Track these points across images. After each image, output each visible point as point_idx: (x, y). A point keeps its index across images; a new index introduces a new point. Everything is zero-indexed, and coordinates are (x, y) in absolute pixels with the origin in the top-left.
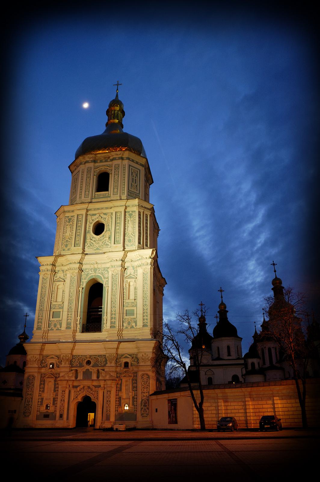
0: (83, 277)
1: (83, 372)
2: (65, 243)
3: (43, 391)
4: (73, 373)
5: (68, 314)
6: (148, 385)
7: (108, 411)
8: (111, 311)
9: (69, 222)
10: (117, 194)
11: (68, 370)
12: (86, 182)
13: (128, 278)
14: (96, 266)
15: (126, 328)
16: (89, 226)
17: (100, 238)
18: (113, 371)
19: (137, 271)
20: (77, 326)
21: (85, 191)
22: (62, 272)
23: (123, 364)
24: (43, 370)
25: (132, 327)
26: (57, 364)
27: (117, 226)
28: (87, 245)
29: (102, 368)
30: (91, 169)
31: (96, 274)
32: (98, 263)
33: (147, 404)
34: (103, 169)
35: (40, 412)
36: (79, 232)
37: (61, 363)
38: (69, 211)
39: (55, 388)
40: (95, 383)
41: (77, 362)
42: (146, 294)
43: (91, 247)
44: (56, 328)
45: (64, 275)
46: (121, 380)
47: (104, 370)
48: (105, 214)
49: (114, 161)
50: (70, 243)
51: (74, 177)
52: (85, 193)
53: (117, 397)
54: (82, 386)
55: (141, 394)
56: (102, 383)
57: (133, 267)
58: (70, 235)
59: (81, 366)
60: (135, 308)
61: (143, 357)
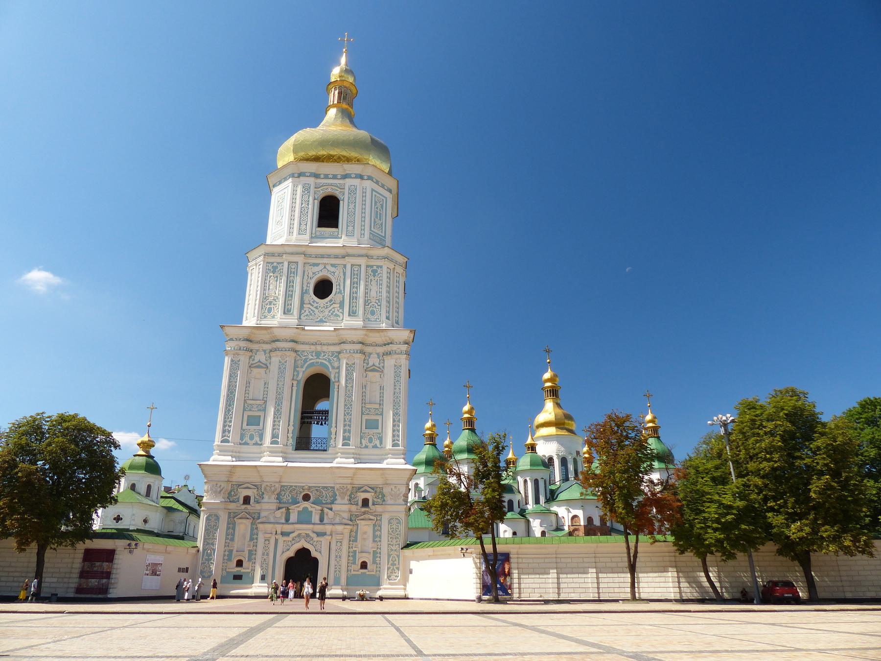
2: (268, 306)
3: (232, 540)
4: (282, 513)
6: (397, 534)
7: (338, 572)
8: (345, 421)
11: (274, 507)
12: (301, 209)
14: (319, 348)
17: (327, 303)
18: (344, 511)
19: (384, 360)
20: (287, 440)
21: (300, 223)
22: (263, 352)
23: (361, 501)
24: (232, 506)
27: (354, 287)
28: (303, 313)
29: (329, 506)
31: (320, 361)
32: (322, 344)
33: (397, 562)
34: (330, 190)
35: (228, 570)
36: (292, 291)
37: (262, 496)
38: (273, 254)
39: (252, 534)
40: (319, 528)
41: (289, 496)
42: (397, 397)
43: (311, 317)
44: (254, 442)
45: (266, 357)
46: (357, 525)
48: (333, 265)
49: (347, 180)
50: (276, 307)
52: (300, 227)
53: (351, 550)
55: (388, 547)
56: (328, 528)
57: (378, 354)
58: (275, 294)
59: (295, 502)
61: (393, 492)
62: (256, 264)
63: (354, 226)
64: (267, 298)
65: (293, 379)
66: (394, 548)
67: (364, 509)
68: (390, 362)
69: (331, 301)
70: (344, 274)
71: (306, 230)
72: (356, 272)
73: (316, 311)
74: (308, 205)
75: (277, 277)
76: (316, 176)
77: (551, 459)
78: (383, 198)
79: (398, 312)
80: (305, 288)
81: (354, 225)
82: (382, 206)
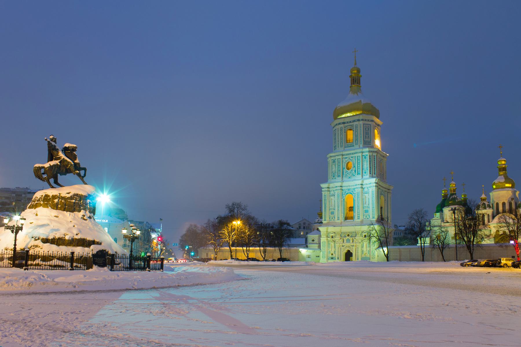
0: (344, 193)
1: (346, 240)
5: (338, 213)
8: (358, 211)
13: (365, 193)
14: (349, 188)
15: (365, 219)
16: (344, 165)
30: (342, 129)
31: (350, 192)
37: (336, 235)
40: (352, 244)
43: (346, 177)
47: (355, 238)
48: (352, 157)
54: (346, 246)
56: (355, 244)
57: (367, 187)
59: (345, 237)
60: (368, 209)
66: (373, 249)
67: (364, 238)
69: (352, 170)
74: (342, 135)
80: (344, 167)
82: (369, 129)
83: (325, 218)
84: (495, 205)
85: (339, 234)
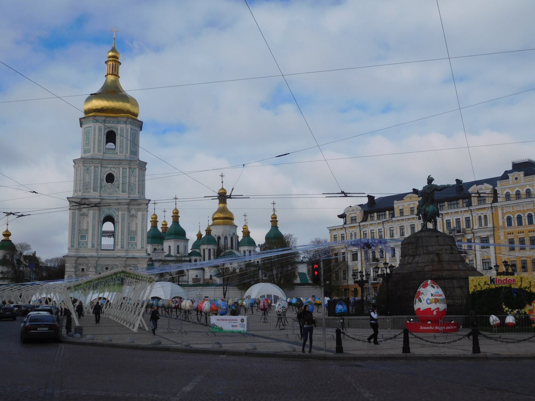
0: (101, 213)
2: (86, 187)
5: (92, 238)
9: (88, 170)
10: (123, 153)
15: (130, 248)
19: (137, 212)
24: (78, 273)
25: (134, 248)
26: (86, 269)
30: (102, 128)
34: (111, 129)
43: (105, 192)
51: (85, 128)
62: (79, 166)
63: (123, 148)
64: (85, 183)
65: (99, 221)
68: (140, 214)
70: (119, 172)
71: (101, 150)
72: (124, 172)
73: (107, 190)
75: (89, 173)
76: (104, 122)
77: (219, 238)
78: (136, 131)
79: (143, 189)
81: (123, 148)
82: (135, 135)
83: (73, 243)
84: (216, 239)
85: (94, 267)
